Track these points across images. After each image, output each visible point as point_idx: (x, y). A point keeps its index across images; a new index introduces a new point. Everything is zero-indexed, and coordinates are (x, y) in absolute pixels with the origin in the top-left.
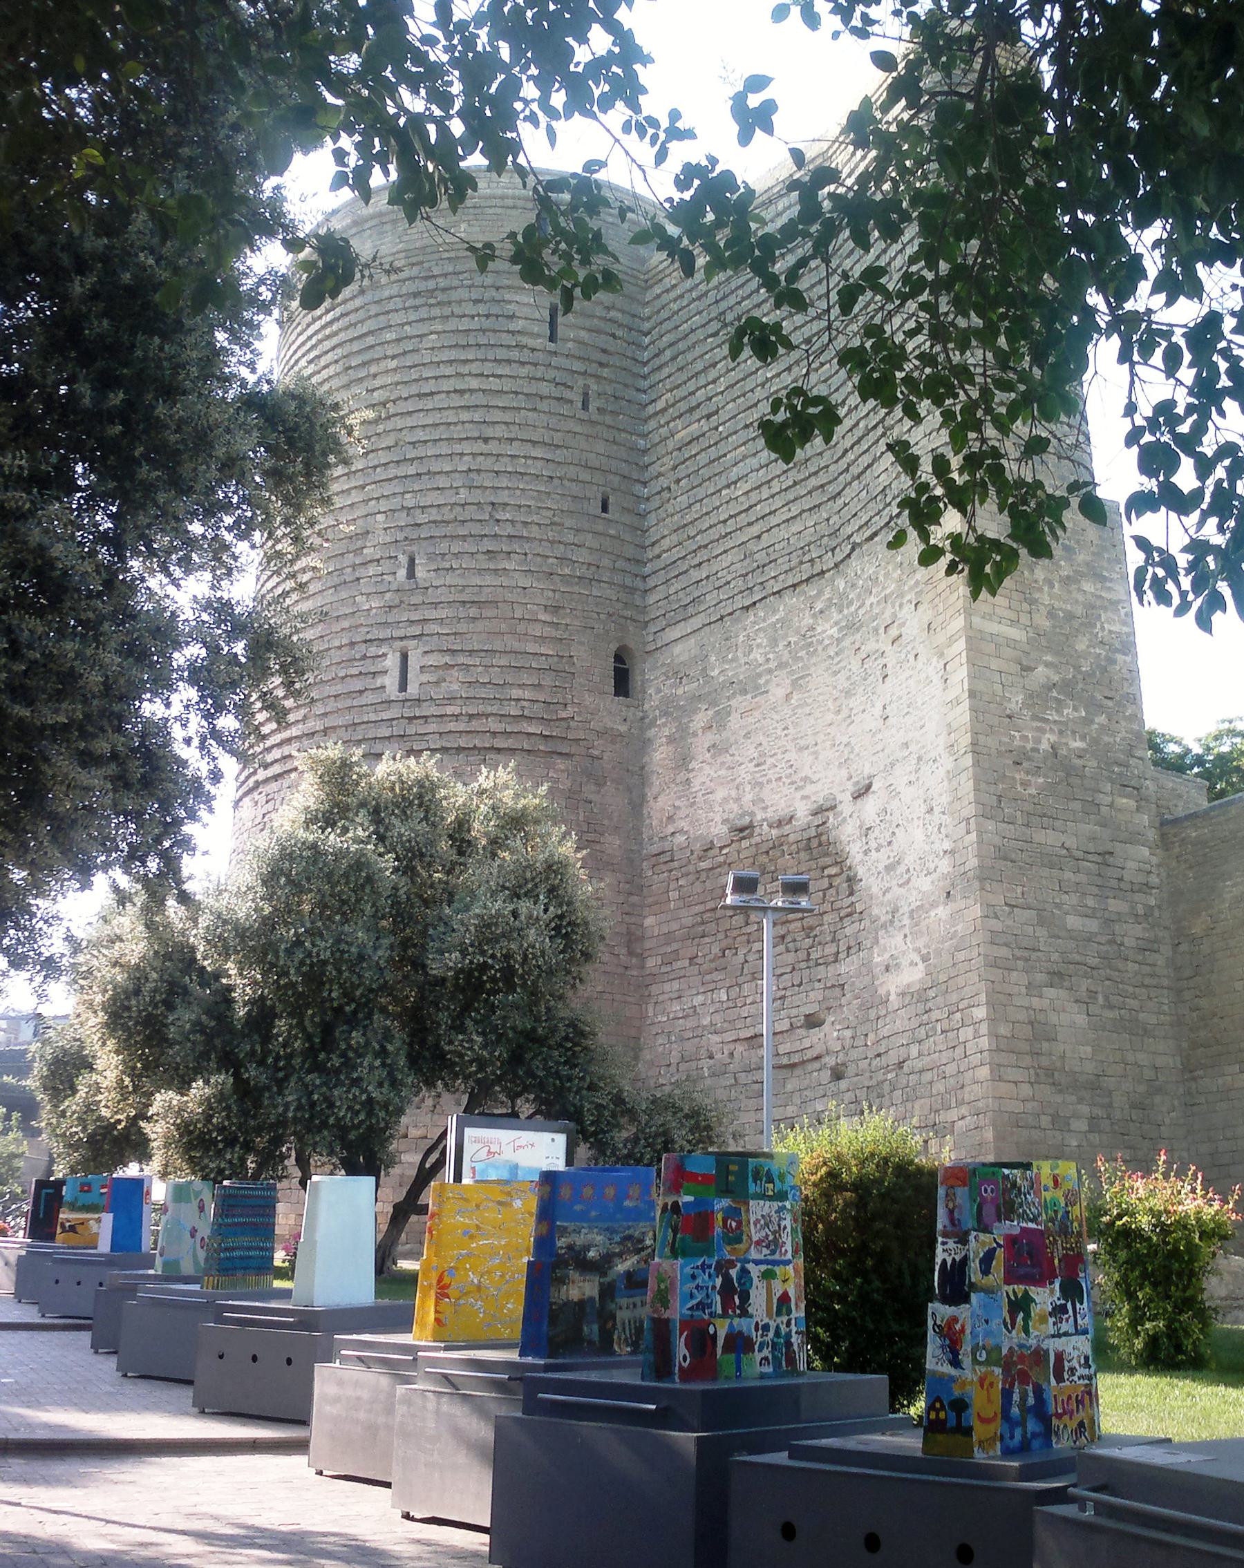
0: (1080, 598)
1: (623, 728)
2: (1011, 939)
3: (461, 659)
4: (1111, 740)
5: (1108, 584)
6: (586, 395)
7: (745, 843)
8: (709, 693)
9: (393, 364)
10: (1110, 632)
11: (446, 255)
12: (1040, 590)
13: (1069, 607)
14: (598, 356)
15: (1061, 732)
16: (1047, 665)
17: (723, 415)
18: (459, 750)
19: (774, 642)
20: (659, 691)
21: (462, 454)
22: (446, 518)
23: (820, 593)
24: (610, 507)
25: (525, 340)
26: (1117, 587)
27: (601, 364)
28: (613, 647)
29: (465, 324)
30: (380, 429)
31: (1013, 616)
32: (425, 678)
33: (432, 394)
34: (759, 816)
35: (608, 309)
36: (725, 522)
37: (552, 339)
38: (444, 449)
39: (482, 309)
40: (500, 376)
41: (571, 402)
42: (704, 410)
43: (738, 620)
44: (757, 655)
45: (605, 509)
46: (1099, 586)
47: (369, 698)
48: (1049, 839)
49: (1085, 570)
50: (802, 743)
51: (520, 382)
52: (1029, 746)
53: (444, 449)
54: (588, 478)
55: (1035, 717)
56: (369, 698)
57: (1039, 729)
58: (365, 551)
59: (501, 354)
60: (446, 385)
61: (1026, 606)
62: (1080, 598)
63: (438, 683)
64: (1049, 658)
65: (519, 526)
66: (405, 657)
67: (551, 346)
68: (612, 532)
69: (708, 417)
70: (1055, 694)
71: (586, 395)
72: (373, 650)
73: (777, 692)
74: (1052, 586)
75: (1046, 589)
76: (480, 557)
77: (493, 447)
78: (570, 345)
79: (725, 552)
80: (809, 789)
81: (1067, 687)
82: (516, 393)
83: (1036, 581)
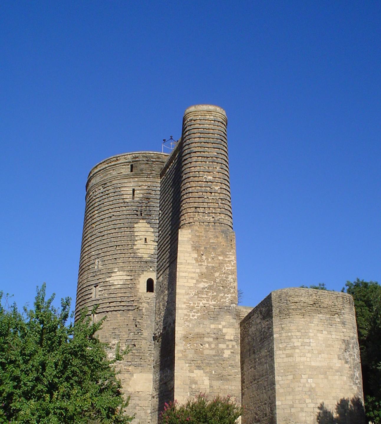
3: (108, 288)
4: (225, 300)
5: (228, 256)
11: (108, 181)
12: (204, 262)
13: (213, 265)
15: (207, 301)
16: (204, 282)
24: (147, 241)
29: (112, 199)
32: (100, 293)
33: (104, 219)
37: (133, 198)
39: (116, 194)
40: (119, 211)
49: (220, 254)
51: (124, 212)
52: (195, 306)
55: (199, 297)
60: (107, 216)
64: (205, 280)
70: (206, 290)
72: (90, 288)
74: (208, 260)
75: (205, 261)
76: (112, 260)
77: (117, 230)
81: (210, 287)
83: (203, 260)
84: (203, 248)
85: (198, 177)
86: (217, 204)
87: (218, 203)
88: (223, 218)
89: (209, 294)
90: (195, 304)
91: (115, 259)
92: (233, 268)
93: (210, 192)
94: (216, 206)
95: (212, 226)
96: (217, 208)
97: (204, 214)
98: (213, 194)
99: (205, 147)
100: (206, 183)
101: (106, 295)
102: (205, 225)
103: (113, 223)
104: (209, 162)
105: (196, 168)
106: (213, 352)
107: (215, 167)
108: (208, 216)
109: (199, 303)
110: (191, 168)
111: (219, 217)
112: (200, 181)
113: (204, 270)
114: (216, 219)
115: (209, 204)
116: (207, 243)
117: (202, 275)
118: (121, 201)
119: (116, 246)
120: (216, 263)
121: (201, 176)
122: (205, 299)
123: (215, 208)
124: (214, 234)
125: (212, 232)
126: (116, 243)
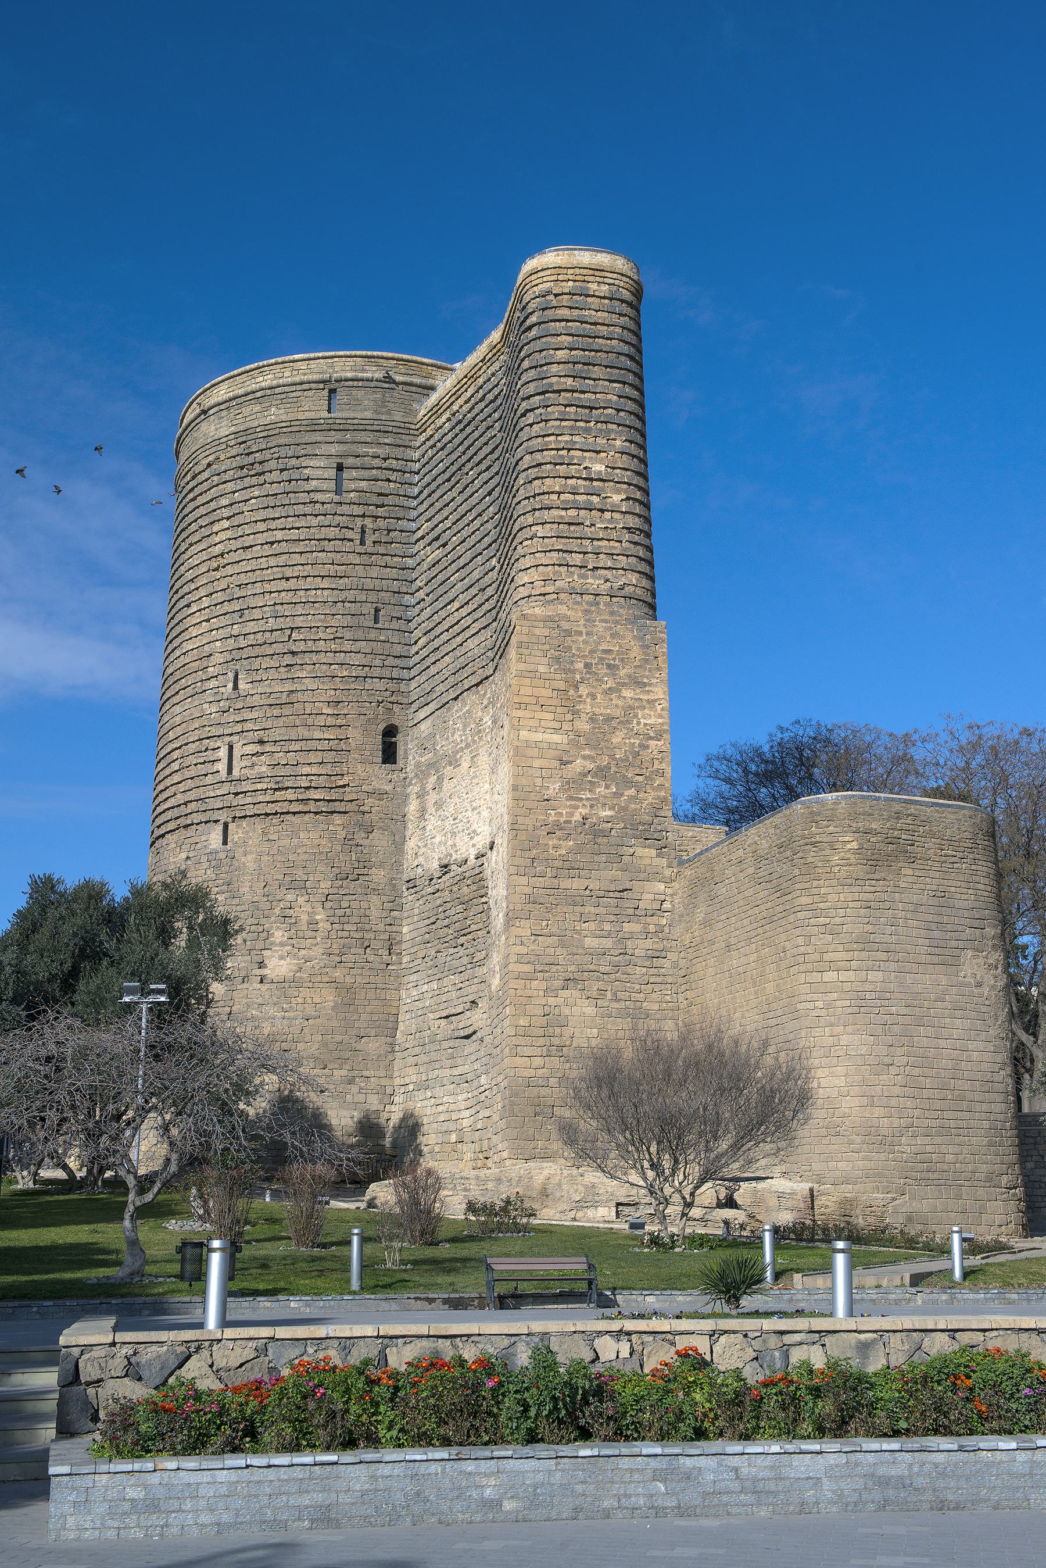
0: (620, 703)
1: (388, 788)
2: (533, 958)
6: (363, 532)
7: (448, 876)
8: (435, 763)
9: (226, 524)
10: (646, 724)
14: (375, 500)
15: (592, 806)
16: (584, 757)
17: (449, 548)
18: (267, 815)
19: (465, 726)
20: (414, 758)
21: (271, 592)
22: (259, 642)
23: (486, 692)
25: (318, 497)
26: (656, 689)
27: (377, 506)
28: (382, 727)
29: (275, 489)
30: (218, 574)
31: (557, 725)
33: (251, 546)
34: (454, 857)
35: (385, 459)
36: (447, 630)
37: (338, 491)
38: (258, 588)
40: (298, 528)
41: (351, 540)
42: (441, 542)
43: (449, 709)
44: (456, 736)
45: (376, 621)
46: (638, 691)
47: (209, 779)
48: (577, 884)
50: (474, 804)
51: (312, 530)
52: (562, 820)
53: (258, 588)
54: (364, 598)
55: (571, 798)
56: (209, 779)
57: (571, 806)
58: (210, 669)
59: (300, 509)
60: (261, 538)
61: (569, 717)
62: (620, 703)
63: (253, 765)
65: (310, 643)
66: (231, 748)
67: (337, 498)
68: (382, 638)
69: (444, 545)
70: (589, 778)
71: (363, 532)
72: (212, 744)
73: (465, 765)
74: (593, 696)
76: (282, 669)
77: (292, 584)
78: (352, 495)
79: (447, 654)
80: (476, 839)
81: (602, 773)
82: (310, 540)
83: (580, 697)
84: (580, 666)
85: (568, 464)
86: (618, 544)
87: (621, 542)
88: (634, 582)
89: (598, 790)
90: (561, 814)
91: (288, 665)
92: (660, 721)
93: (599, 510)
94: (615, 548)
95: (605, 604)
96: (618, 555)
97: (583, 570)
98: (607, 515)
99: (585, 378)
100: (588, 483)
101: (264, 769)
102: (588, 603)
103: (282, 560)
104: (597, 422)
105: (559, 438)
106: (608, 943)
107: (613, 436)
108: (594, 577)
109: (572, 814)
110: (547, 439)
111: (623, 580)
112: (573, 477)
113: (582, 725)
114: (616, 586)
115: (595, 543)
116: (592, 652)
117: (577, 739)
118: (304, 497)
119: (292, 629)
120: (617, 706)
121: (575, 461)
122: (584, 802)
123: (613, 554)
124: (611, 628)
125: (606, 621)
126: (289, 623)
